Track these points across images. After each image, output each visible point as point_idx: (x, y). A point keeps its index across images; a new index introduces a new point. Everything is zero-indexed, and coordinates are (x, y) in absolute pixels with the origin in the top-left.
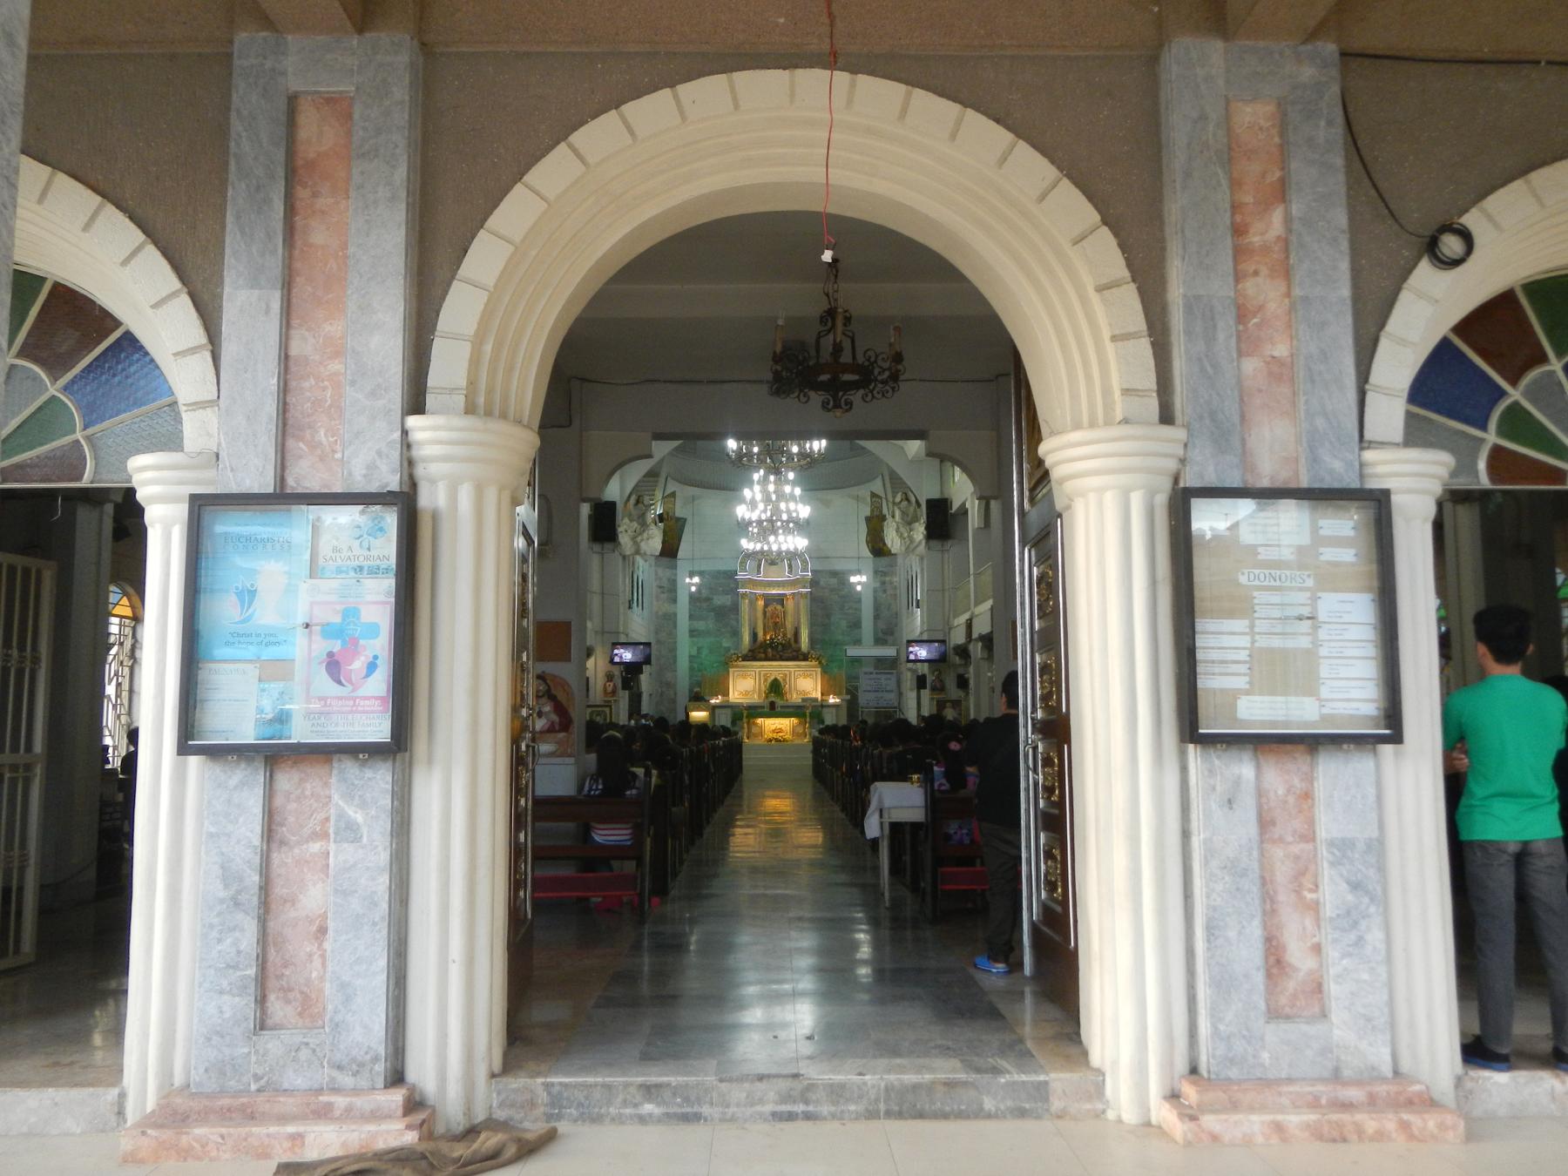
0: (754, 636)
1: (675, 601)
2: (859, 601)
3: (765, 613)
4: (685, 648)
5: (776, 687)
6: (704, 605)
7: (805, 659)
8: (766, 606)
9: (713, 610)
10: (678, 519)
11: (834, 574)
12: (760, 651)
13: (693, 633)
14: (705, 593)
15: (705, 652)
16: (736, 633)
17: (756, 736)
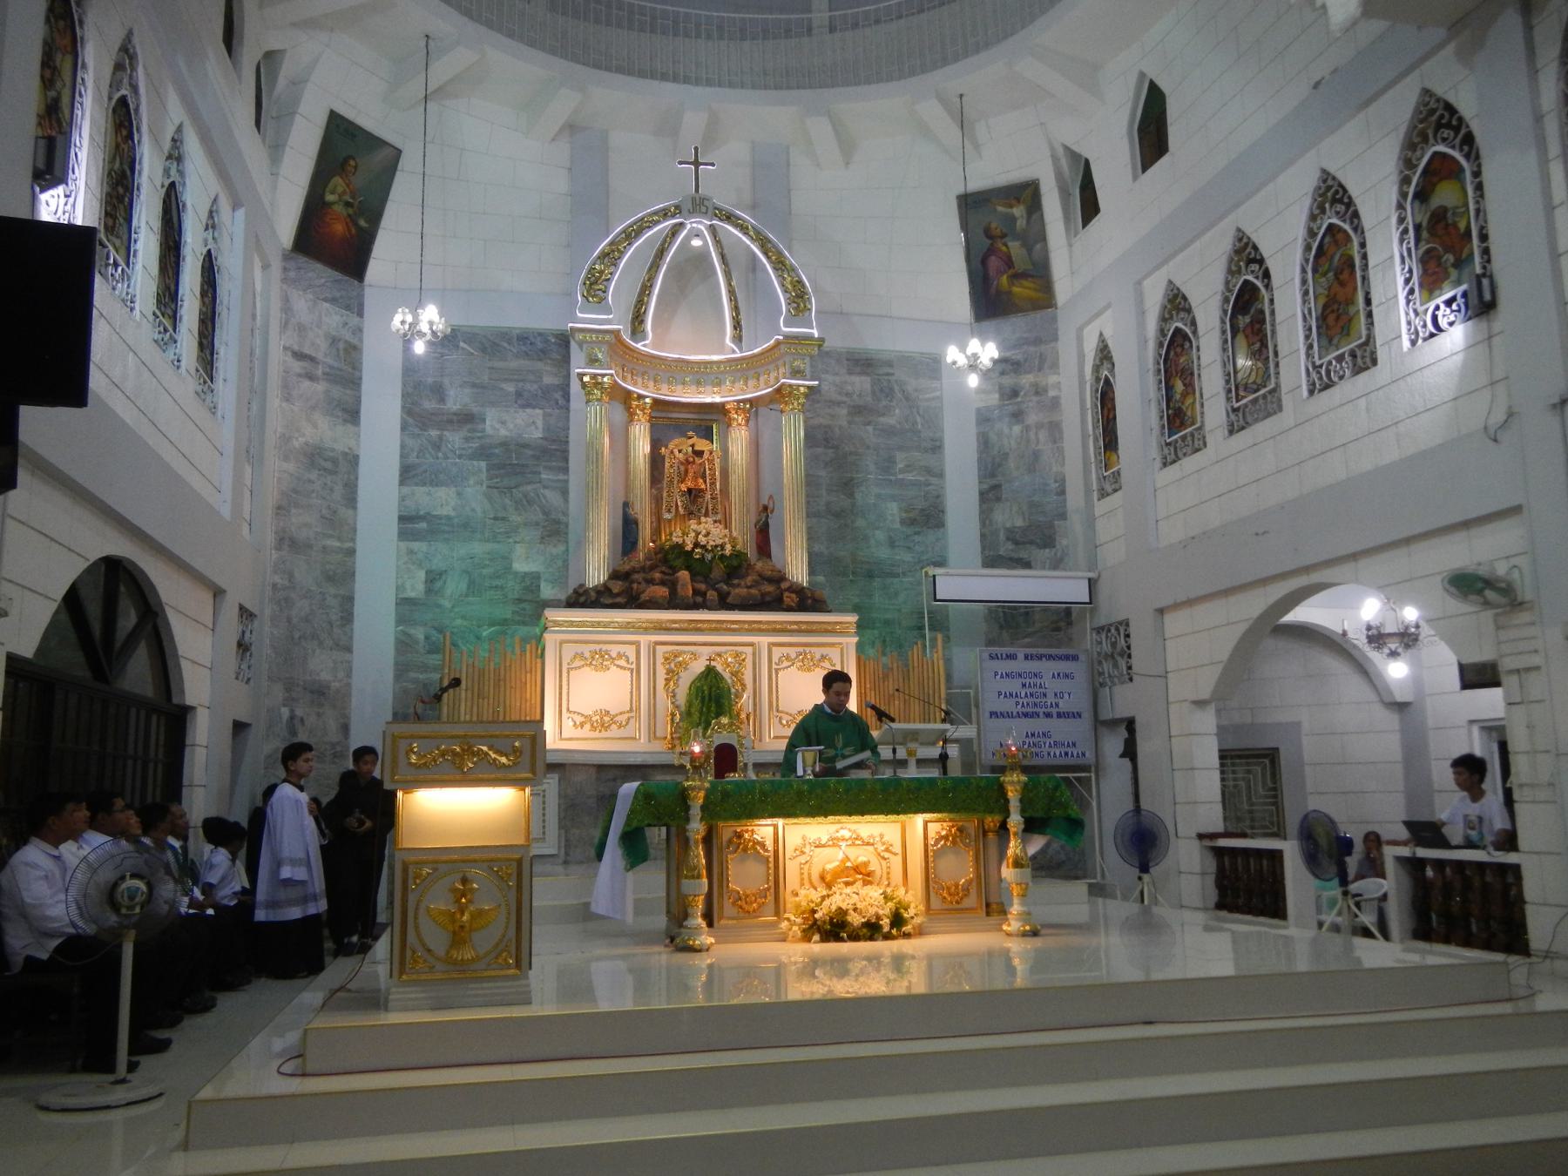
0: (628, 529)
1: (352, 414)
2: (936, 448)
3: (656, 461)
4: (381, 573)
5: (711, 697)
6: (455, 438)
7: (807, 601)
8: (656, 444)
9: (483, 453)
10: (374, 142)
11: (862, 363)
12: (656, 576)
13: (411, 524)
14: (458, 399)
15: (454, 586)
16: (555, 529)
17: (746, 908)
